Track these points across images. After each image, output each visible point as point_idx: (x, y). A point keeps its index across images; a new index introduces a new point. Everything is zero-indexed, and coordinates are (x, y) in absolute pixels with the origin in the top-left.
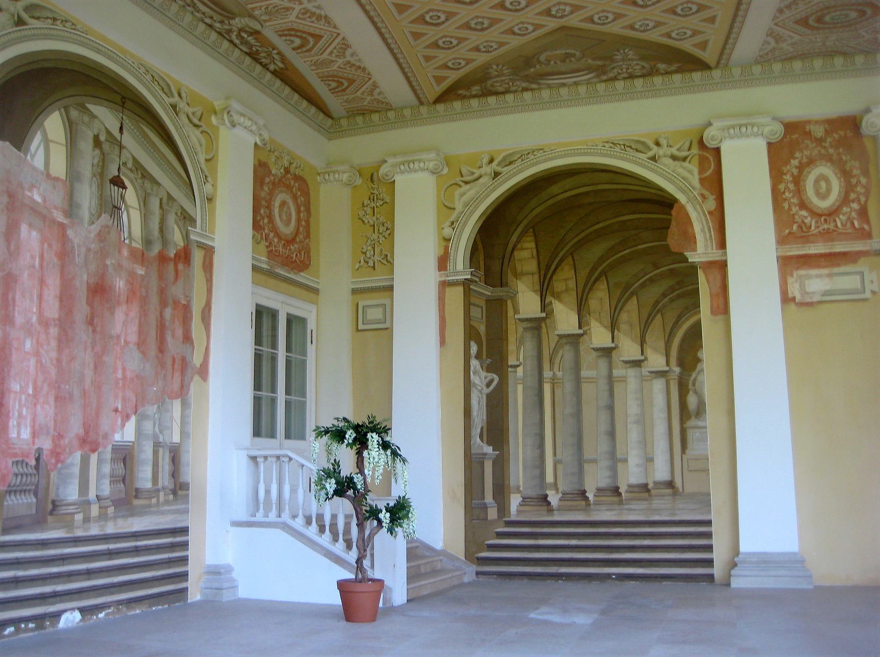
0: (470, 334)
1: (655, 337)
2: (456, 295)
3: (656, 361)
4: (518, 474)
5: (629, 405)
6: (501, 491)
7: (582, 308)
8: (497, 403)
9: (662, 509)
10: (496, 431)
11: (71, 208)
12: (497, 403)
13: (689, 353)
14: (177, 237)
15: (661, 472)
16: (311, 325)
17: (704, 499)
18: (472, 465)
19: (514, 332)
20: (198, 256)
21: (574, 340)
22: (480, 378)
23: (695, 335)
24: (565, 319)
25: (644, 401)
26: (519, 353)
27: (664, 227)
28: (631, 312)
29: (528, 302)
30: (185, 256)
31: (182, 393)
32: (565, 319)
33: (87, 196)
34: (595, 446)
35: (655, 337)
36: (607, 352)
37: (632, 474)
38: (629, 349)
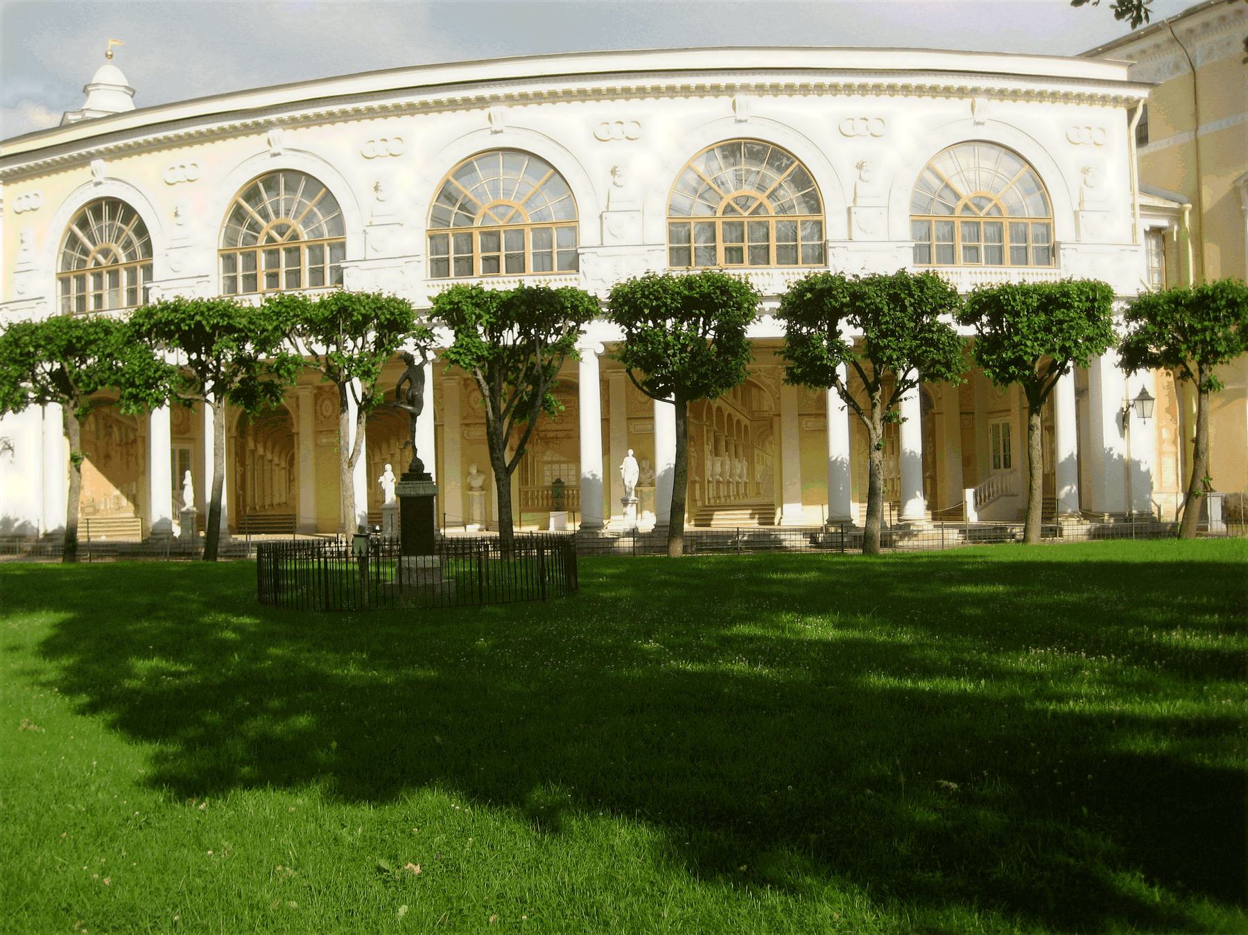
0: (236, 454)
1: (283, 456)
2: (233, 441)
3: (283, 464)
4: (249, 500)
5: (276, 478)
6: (245, 507)
7: (265, 448)
8: (243, 476)
9: (284, 511)
10: (243, 487)
11: (98, 438)
12: (243, 476)
13: (291, 462)
14: (131, 436)
15: (283, 499)
16: (192, 451)
17: (294, 508)
18: (238, 497)
19: (248, 454)
20: (139, 440)
21: (262, 457)
22: (239, 469)
23: (293, 456)
24: (261, 451)
25: (280, 476)
26: (249, 461)
27: (285, 420)
28: (277, 450)
29: (251, 445)
30: (135, 441)
31: (136, 480)
32: (261, 451)
33: (102, 433)
34: (268, 492)
35: (283, 456)
36: (271, 461)
37: (276, 501)
38: (276, 461)
